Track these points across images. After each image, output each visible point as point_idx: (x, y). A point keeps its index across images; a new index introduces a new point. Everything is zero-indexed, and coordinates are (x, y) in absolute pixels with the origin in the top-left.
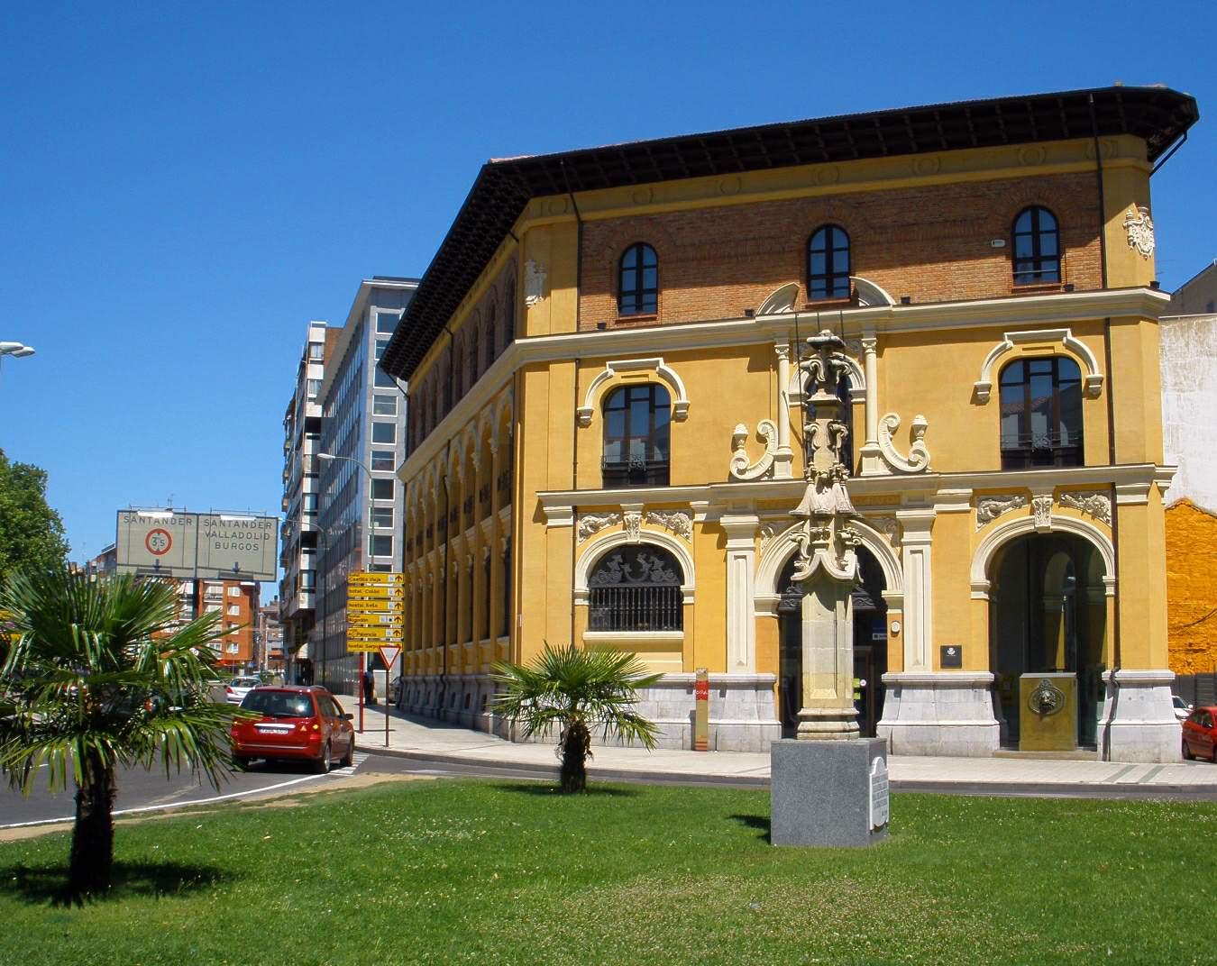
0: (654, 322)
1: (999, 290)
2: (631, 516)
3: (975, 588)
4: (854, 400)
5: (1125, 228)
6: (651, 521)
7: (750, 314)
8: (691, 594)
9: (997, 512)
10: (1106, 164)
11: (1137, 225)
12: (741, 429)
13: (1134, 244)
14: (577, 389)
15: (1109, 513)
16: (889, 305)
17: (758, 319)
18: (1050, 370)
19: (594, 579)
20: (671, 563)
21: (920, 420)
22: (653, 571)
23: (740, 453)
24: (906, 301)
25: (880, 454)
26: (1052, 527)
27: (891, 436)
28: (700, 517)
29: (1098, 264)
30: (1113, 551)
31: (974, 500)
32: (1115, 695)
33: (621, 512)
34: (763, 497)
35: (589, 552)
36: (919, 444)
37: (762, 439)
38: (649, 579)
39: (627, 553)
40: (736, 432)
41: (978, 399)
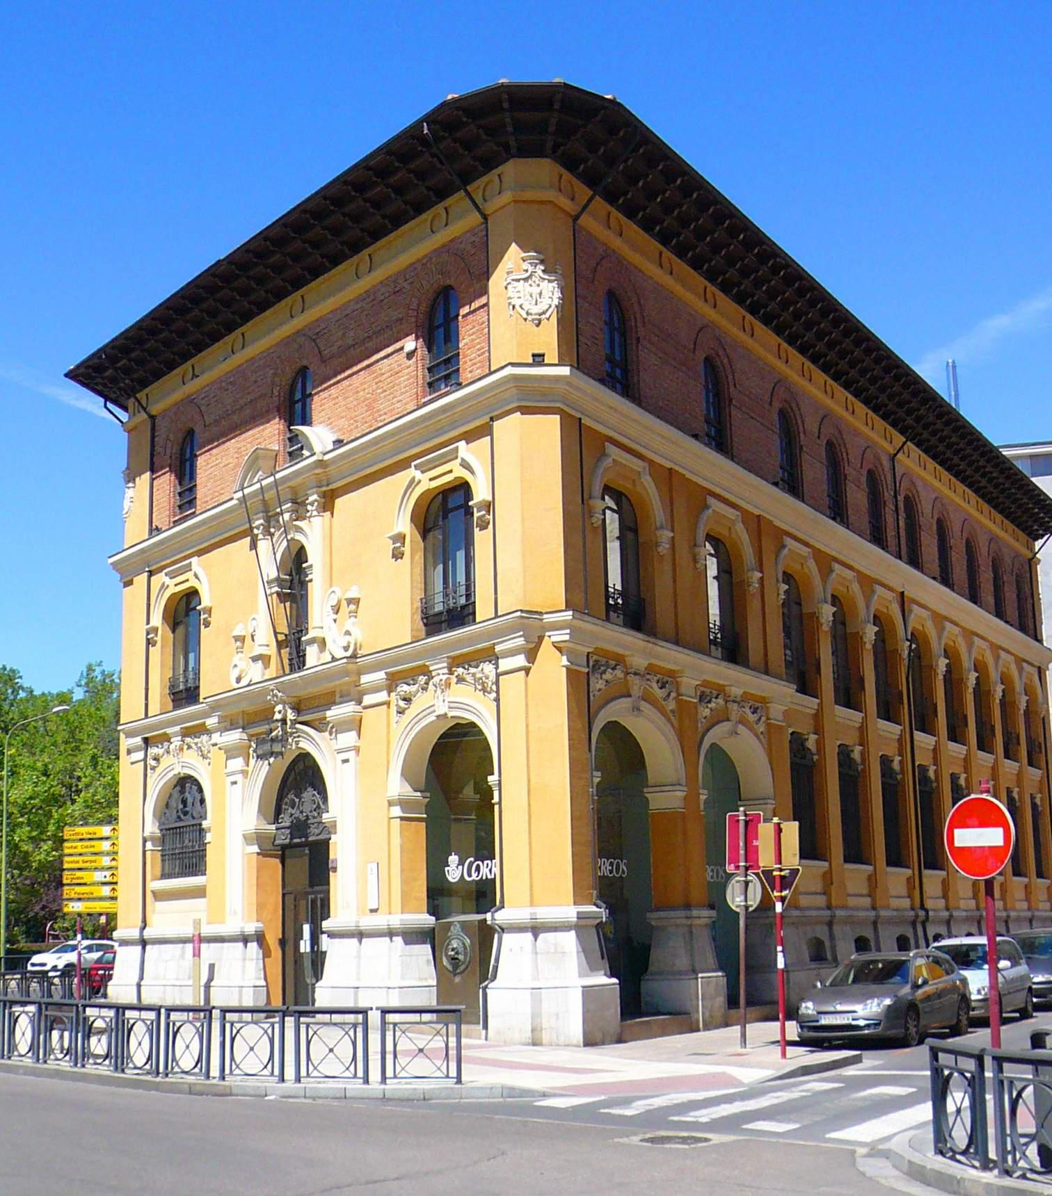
1: (411, 407)
2: (176, 741)
3: (391, 804)
9: (407, 700)
10: (489, 208)
11: (518, 280)
12: (238, 632)
21: (352, 594)
27: (335, 616)
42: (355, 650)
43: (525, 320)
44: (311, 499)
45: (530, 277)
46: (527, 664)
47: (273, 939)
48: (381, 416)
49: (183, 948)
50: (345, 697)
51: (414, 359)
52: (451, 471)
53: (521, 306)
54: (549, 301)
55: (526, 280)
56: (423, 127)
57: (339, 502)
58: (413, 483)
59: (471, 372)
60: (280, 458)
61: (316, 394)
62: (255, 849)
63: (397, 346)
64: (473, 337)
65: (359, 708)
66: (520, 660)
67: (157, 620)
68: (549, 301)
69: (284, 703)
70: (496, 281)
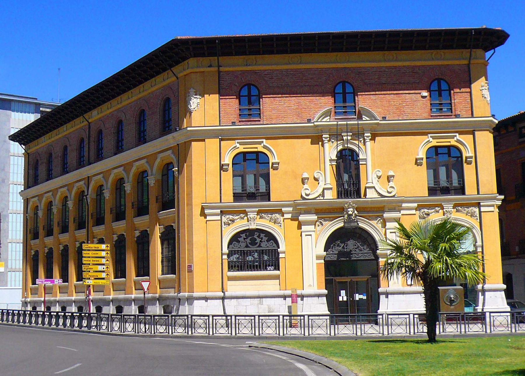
2: (251, 215)
5: (481, 90)
6: (261, 218)
7: (309, 121)
8: (284, 253)
12: (305, 175)
13: (485, 98)
15: (478, 216)
18: (447, 152)
19: (231, 246)
20: (271, 238)
21: (391, 173)
22: (262, 242)
23: (306, 186)
24: (384, 118)
25: (374, 187)
27: (378, 180)
28: (289, 216)
30: (480, 232)
31: (418, 208)
32: (484, 295)
34: (320, 207)
35: (229, 233)
36: (391, 184)
37: (316, 180)
38: (260, 246)
39: (249, 232)
40: (303, 177)
41: (418, 162)
48: (405, 113)
49: (260, 300)
50: (392, 210)
51: (426, 99)
63: (419, 91)
67: (228, 160)
69: (353, 207)
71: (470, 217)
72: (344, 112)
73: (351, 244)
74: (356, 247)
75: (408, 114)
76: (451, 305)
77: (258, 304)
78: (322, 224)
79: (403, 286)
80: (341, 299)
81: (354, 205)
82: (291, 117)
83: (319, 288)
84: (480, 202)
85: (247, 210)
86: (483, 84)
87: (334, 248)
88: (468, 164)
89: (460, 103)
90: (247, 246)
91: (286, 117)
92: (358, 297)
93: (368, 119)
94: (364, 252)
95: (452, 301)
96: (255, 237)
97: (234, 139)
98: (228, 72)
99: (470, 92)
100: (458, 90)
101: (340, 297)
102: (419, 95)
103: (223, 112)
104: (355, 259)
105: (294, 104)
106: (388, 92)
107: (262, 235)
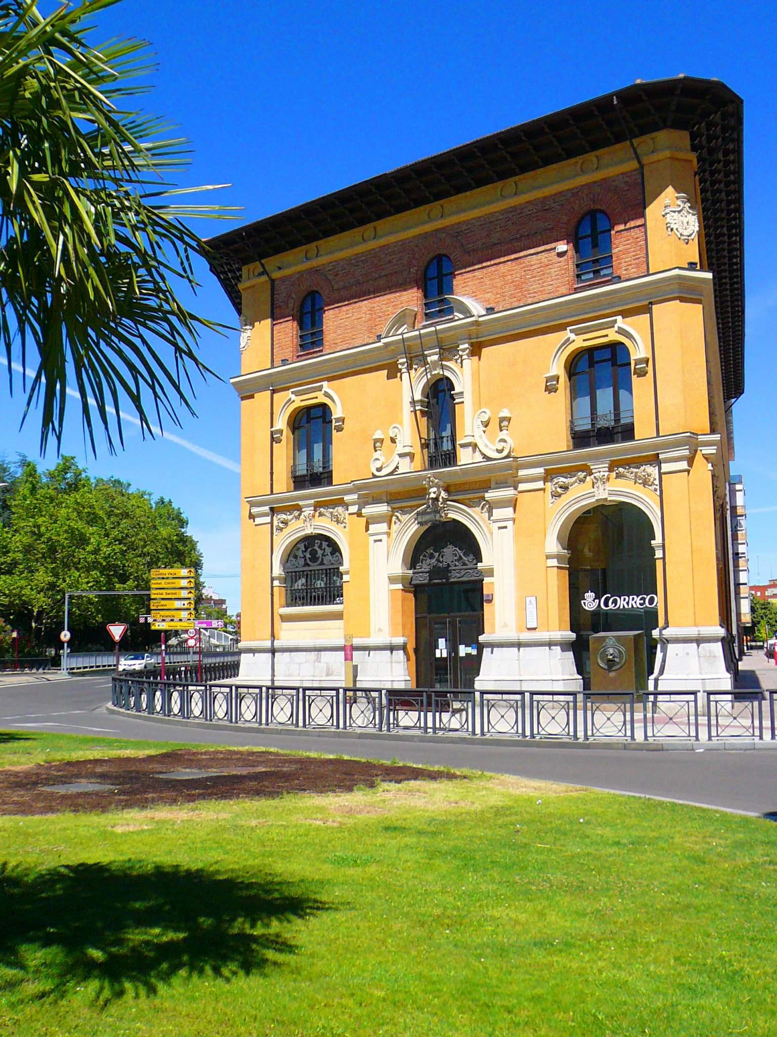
0: (321, 354)
1: (563, 290)
2: (308, 511)
3: (548, 557)
4: (457, 401)
5: (664, 216)
6: (321, 515)
8: (347, 573)
9: (565, 488)
10: (645, 160)
11: (674, 212)
12: (378, 435)
14: (272, 414)
15: (657, 482)
16: (474, 316)
17: (384, 341)
19: (289, 564)
20: (335, 548)
21: (505, 413)
23: (377, 455)
24: (490, 310)
25: (475, 446)
26: (609, 499)
27: (484, 429)
28: (354, 509)
29: (643, 254)
31: (548, 476)
32: (664, 651)
33: (299, 508)
34: (393, 489)
35: (283, 541)
36: (504, 435)
38: (322, 563)
39: (309, 541)
42: (509, 452)
43: (680, 239)
44: (461, 347)
45: (681, 211)
46: (687, 468)
47: (411, 647)
48: (529, 294)
51: (565, 257)
52: (607, 336)
53: (677, 229)
54: (693, 228)
55: (679, 212)
56: (613, 99)
57: (485, 351)
58: (568, 342)
59: (625, 270)
60: (419, 317)
61: (458, 274)
62: (400, 586)
64: (629, 246)
65: (516, 492)
66: (684, 465)
67: (281, 423)
68: (693, 228)
69: (437, 486)
70: (653, 211)
71: (642, 485)
72: (440, 311)
73: (450, 553)
74: (456, 558)
75: (535, 295)
76: (610, 669)
77: (314, 662)
78: (399, 520)
79: (520, 630)
80: (438, 655)
81: (437, 481)
82: (361, 335)
83: (394, 635)
84: (658, 454)
85: (301, 503)
86: (667, 201)
87: (424, 562)
88: (639, 376)
89: (626, 252)
90: (306, 565)
91: (354, 337)
92: (463, 650)
93: (461, 316)
94: (468, 567)
95: (611, 663)
96: (316, 548)
97: (287, 389)
98: (283, 279)
99: (644, 225)
100: (622, 227)
101: (437, 650)
102: (553, 253)
103: (277, 346)
104: (455, 580)
105: (365, 313)
106: (502, 259)
107: (325, 544)
